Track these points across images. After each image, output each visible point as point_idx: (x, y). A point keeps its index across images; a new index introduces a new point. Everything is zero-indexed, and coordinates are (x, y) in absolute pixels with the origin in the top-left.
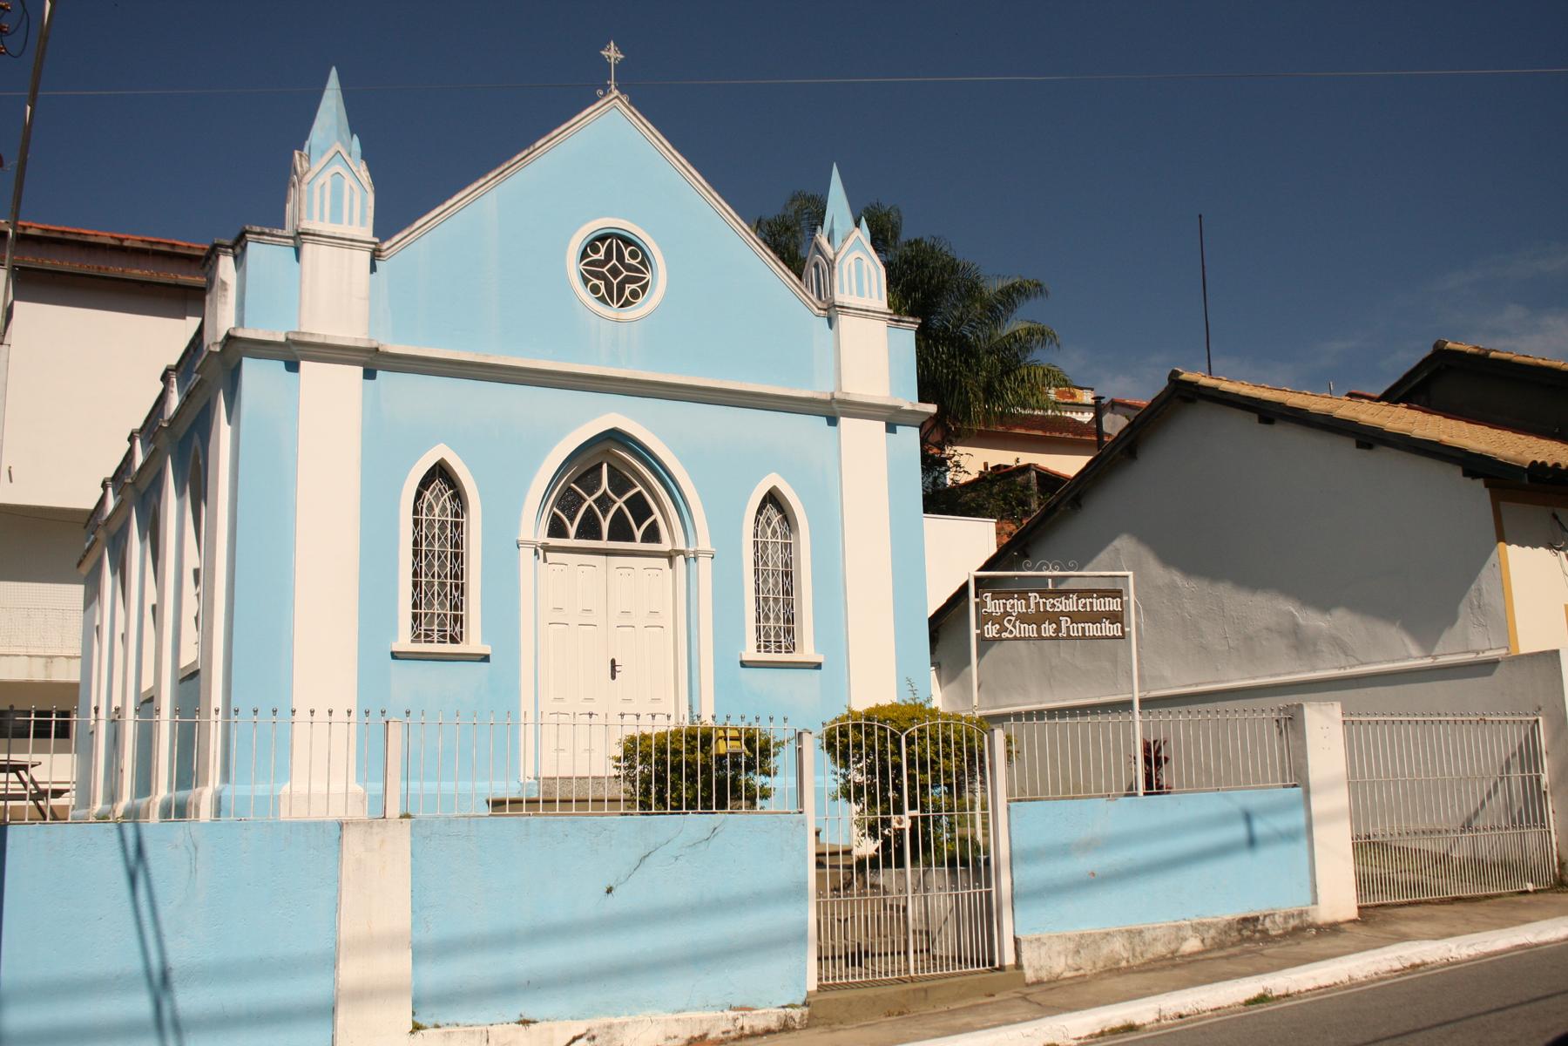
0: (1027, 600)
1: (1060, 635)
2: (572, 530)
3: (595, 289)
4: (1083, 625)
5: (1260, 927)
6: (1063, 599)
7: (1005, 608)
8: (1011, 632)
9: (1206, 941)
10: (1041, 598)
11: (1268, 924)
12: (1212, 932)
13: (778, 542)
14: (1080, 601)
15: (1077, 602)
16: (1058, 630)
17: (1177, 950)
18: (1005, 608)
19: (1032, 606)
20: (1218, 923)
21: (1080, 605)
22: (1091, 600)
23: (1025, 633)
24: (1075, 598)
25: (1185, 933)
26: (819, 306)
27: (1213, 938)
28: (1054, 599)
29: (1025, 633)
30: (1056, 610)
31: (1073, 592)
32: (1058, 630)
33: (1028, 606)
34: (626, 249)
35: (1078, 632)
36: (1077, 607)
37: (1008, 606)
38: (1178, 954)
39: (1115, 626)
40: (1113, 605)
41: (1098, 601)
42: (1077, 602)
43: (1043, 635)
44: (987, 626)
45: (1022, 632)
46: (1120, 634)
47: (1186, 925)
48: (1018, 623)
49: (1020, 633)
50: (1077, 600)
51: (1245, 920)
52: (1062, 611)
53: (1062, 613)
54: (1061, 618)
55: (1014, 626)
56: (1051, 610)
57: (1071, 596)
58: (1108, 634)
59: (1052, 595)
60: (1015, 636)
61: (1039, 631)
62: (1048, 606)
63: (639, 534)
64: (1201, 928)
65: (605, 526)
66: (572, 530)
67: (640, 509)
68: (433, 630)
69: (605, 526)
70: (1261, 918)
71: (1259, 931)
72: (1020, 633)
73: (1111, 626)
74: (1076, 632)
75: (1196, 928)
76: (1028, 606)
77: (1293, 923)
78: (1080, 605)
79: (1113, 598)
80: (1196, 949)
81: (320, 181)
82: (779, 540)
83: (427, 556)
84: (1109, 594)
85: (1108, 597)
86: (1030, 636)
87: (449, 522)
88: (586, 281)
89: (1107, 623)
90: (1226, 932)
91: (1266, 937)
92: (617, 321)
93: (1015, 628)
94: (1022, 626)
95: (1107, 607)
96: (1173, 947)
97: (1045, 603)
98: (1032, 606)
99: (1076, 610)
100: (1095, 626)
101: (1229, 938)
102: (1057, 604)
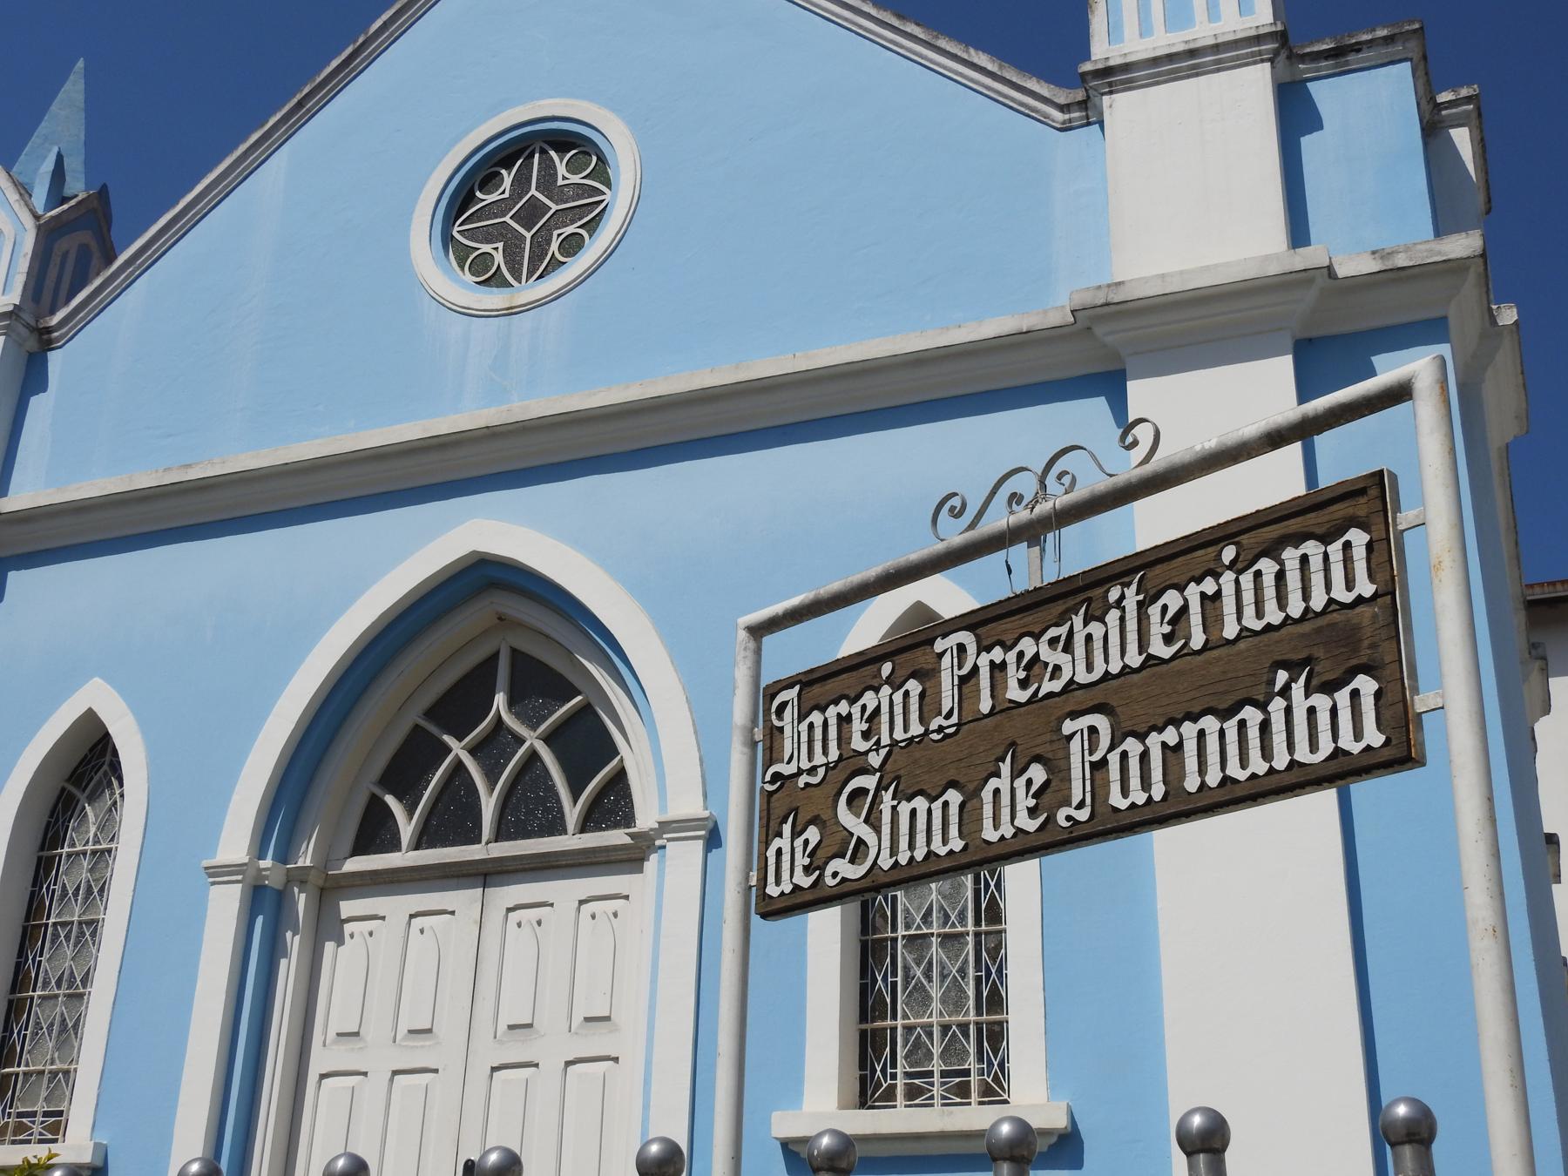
0: (928, 675)
2: (407, 829)
4: (1170, 736)
6: (1078, 621)
7: (843, 740)
10: (984, 648)
14: (1154, 611)
15: (1142, 619)
18: (843, 740)
21: (1158, 629)
23: (912, 846)
24: (1132, 599)
26: (1062, 100)
28: (1037, 637)
29: (912, 846)
30: (1048, 686)
31: (1119, 572)
32: (1048, 796)
34: (561, 161)
35: (1146, 784)
36: (1143, 645)
37: (858, 726)
39: (1343, 697)
41: (1247, 579)
42: (1142, 619)
45: (904, 843)
46: (1375, 738)
48: (887, 796)
49: (894, 851)
50: (1140, 604)
53: (1078, 699)
54: (1068, 727)
55: (872, 820)
56: (1023, 696)
57: (1114, 595)
58: (1303, 754)
59: (1028, 619)
61: (969, 816)
63: (572, 814)
65: (489, 806)
66: (407, 829)
68: (34, 1114)
69: (489, 806)
72: (894, 851)
73: (1321, 702)
78: (1158, 629)
79: (1326, 539)
84: (1293, 525)
85: (1298, 539)
88: (555, 264)
89: (1298, 689)
92: (510, 312)
93: (877, 830)
94: (905, 808)
95: (1271, 605)
100: (1231, 726)
102: (1050, 656)
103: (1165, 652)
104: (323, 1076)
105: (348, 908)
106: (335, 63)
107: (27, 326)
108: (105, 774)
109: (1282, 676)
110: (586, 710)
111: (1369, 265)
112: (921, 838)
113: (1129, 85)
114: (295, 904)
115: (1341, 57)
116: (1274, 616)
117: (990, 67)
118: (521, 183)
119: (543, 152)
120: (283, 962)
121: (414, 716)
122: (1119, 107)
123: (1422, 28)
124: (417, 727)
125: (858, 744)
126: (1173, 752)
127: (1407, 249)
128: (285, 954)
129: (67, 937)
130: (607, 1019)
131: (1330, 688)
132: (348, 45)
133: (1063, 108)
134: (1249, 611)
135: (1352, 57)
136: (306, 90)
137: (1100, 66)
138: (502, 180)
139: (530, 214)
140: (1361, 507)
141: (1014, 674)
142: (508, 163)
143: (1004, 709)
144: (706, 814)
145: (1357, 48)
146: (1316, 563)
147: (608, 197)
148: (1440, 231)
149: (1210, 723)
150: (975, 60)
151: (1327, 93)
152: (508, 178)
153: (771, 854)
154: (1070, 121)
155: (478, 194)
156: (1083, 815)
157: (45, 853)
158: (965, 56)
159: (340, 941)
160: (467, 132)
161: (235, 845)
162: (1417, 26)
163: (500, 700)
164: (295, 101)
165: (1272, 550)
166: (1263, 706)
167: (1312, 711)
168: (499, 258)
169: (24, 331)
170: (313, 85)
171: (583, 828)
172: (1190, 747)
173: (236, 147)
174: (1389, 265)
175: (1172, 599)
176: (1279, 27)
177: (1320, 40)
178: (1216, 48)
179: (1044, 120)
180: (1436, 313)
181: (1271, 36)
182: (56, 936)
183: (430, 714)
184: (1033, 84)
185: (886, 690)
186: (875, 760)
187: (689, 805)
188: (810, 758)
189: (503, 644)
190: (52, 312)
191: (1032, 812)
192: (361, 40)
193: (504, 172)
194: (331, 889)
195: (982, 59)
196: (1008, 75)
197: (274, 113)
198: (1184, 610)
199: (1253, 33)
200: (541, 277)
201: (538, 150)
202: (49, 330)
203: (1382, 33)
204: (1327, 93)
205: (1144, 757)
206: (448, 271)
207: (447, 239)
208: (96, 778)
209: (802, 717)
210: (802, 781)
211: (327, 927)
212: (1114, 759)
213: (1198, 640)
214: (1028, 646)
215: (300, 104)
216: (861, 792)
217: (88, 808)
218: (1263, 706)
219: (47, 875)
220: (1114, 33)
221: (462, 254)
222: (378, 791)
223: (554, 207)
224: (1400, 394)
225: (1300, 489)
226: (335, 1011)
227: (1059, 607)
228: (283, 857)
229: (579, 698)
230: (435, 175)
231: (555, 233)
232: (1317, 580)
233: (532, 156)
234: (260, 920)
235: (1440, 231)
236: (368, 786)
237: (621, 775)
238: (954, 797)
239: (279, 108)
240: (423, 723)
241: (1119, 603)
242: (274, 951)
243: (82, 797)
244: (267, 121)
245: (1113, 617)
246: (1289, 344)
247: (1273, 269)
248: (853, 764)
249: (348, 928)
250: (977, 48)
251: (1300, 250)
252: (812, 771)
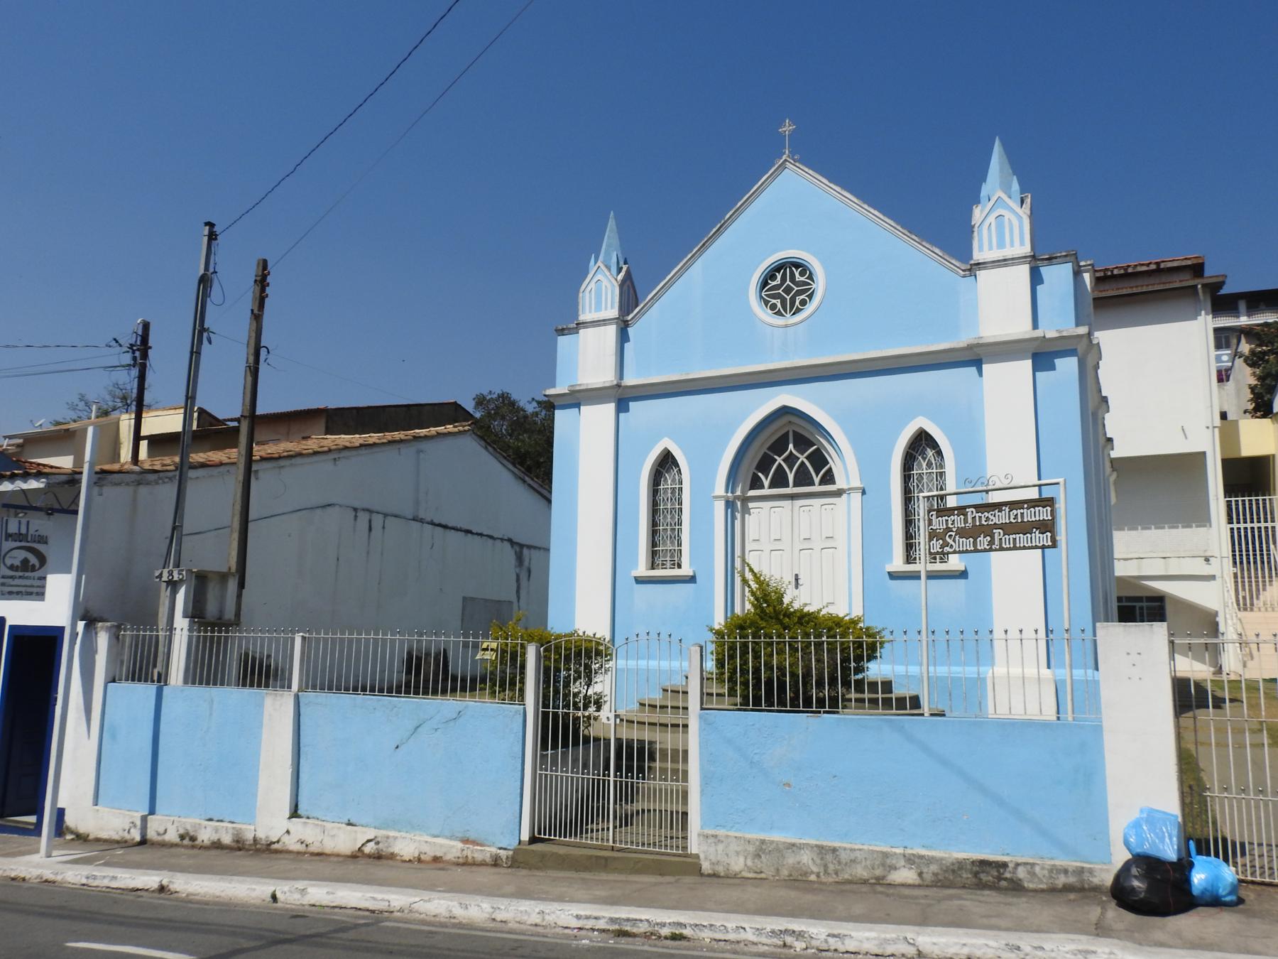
0: (965, 515)
1: (993, 547)
2: (766, 483)
3: (803, 303)
4: (1014, 536)
5: (1008, 875)
6: (997, 511)
7: (947, 524)
8: (952, 546)
9: (925, 875)
10: (977, 512)
11: (1021, 873)
12: (934, 868)
13: (933, 473)
14: (1011, 513)
16: (991, 543)
17: (884, 877)
18: (947, 524)
19: (970, 520)
20: (942, 859)
21: (1012, 517)
22: (1022, 511)
23: (963, 547)
24: (1007, 510)
25: (894, 862)
26: (963, 268)
27: (935, 874)
29: (963, 547)
30: (990, 523)
31: (1005, 504)
32: (991, 543)
33: (966, 521)
35: (1009, 544)
36: (1009, 519)
37: (950, 522)
38: (885, 882)
39: (1045, 535)
40: (1043, 514)
41: (1029, 511)
43: (1004, 546)
44: (979, 539)
45: (961, 546)
46: (1050, 543)
47: (895, 854)
48: (957, 537)
49: (959, 547)
50: (1009, 512)
51: (983, 863)
52: (995, 524)
53: (996, 526)
54: (994, 531)
55: (954, 541)
56: (985, 523)
57: (1004, 508)
58: (1038, 544)
60: (1043, 545)
61: (975, 544)
62: (983, 519)
63: (817, 480)
64: (916, 860)
65: (791, 477)
66: (766, 483)
67: (819, 460)
68: (666, 561)
69: (791, 477)
70: (1011, 865)
71: (1006, 879)
72: (959, 547)
73: (1041, 535)
74: (1007, 543)
75: (911, 860)
76: (966, 521)
77: (1062, 880)
78: (1012, 517)
79: (1044, 507)
80: (910, 882)
81: (589, 288)
82: (934, 471)
83: (663, 512)
85: (1038, 506)
86: (967, 550)
89: (1037, 532)
90: (953, 871)
91: (1016, 887)
92: (786, 326)
93: (955, 542)
94: (961, 540)
96: (878, 872)
97: (980, 517)
98: (970, 520)
99: (1008, 522)
100: (1025, 536)
101: (959, 879)
102: (992, 517)
103: (1014, 521)
104: (750, 551)
105: (751, 505)
106: (714, 230)
107: (622, 321)
109: (1034, 530)
110: (818, 449)
111: (1055, 335)
112: (965, 546)
113: (985, 268)
114: (737, 505)
115: (1050, 260)
116: (1034, 519)
117: (940, 254)
118: (784, 279)
119: (790, 268)
120: (736, 521)
121: (764, 450)
122: (982, 274)
123: (1076, 253)
124: (765, 453)
125: (950, 526)
126: (1015, 539)
127: (1066, 330)
128: (736, 519)
129: (667, 512)
130: (832, 537)
131: (1043, 533)
133: (963, 270)
134: (1029, 517)
135: (1054, 260)
136: (705, 240)
137: (976, 262)
139: (788, 290)
140: (1049, 503)
141: (983, 519)
143: (981, 525)
144: (862, 486)
145: (1056, 258)
146: (1041, 511)
147: (814, 286)
148: (1077, 325)
149: (1021, 535)
150: (935, 251)
151: (1046, 271)
152: (779, 276)
153: (931, 544)
155: (769, 281)
156: (998, 547)
159: (750, 514)
160: (765, 259)
161: (720, 489)
162: (1074, 252)
163: (791, 446)
165: (1034, 507)
166: (1031, 534)
167: (1039, 537)
168: (779, 305)
169: (620, 322)
171: (820, 484)
172: (1018, 539)
173: (683, 259)
174: (1061, 335)
175: (1015, 512)
176: (1032, 254)
177: (1045, 255)
178: (1013, 259)
179: (957, 273)
180: (1075, 347)
181: (1030, 256)
182: (663, 512)
183: (769, 449)
184: (953, 262)
185: (956, 516)
186: (954, 530)
187: (856, 483)
188: (939, 526)
189: (791, 429)
190: (628, 315)
191: (988, 545)
192: (723, 222)
193: (777, 274)
194: (745, 500)
195: (937, 251)
196: (945, 257)
198: (1017, 514)
199: (1024, 255)
200: (794, 314)
202: (628, 321)
203: (1064, 254)
204: (1046, 271)
205: (1009, 539)
206: (761, 307)
207: (761, 297)
208: (667, 466)
209: (937, 518)
210: (938, 531)
211: (746, 511)
212: (1003, 538)
213: (1019, 520)
214: (986, 514)
215: (704, 244)
216: (952, 535)
217: (666, 475)
218: (1031, 534)
219: (657, 494)
220: (981, 249)
221: (766, 303)
222: (756, 472)
224: (1058, 484)
225: (1037, 497)
226: (751, 533)
227: (992, 508)
228: (732, 493)
229: (815, 447)
230: (755, 276)
231: (797, 298)
232: (1041, 515)
233: (786, 269)
234: (729, 510)
235: (1077, 325)
236: (753, 470)
237: (830, 469)
238: (971, 540)
239: (697, 245)
240: (767, 451)
241: (1005, 510)
242: (733, 518)
243: (664, 472)
244: (693, 250)
245: (1003, 512)
246: (1030, 356)
247: (1027, 336)
248: (948, 530)
249: (751, 510)
250: (935, 246)
251: (1036, 331)
252: (940, 529)
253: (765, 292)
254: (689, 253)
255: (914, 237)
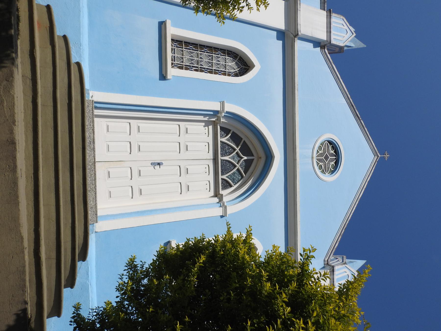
34: (333, 163)
63: (224, 177)
65: (227, 158)
68: (174, 54)
69: (227, 158)
81: (345, 24)
83: (209, 56)
87: (225, 70)
92: (312, 158)
104: (179, 125)
105: (211, 127)
106: (358, 113)
107: (327, 44)
108: (240, 66)
119: (336, 158)
120: (203, 117)
121: (244, 139)
129: (210, 59)
132: (360, 116)
133: (328, 260)
136: (355, 107)
138: (332, 151)
142: (335, 152)
147: (327, 174)
154: (325, 261)
157: (226, 52)
158: (338, 242)
159: (204, 126)
163: (245, 158)
164: (353, 105)
170: (355, 109)
179: (326, 257)
190: (328, 50)
192: (360, 119)
194: (214, 124)
195: (337, 245)
197: (352, 100)
201: (336, 157)
202: (324, 48)
211: (207, 124)
215: (352, 106)
219: (222, 52)
222: (231, 132)
223: (327, 162)
226: (192, 127)
229: (244, 175)
233: (335, 156)
234: (212, 113)
242: (205, 115)
243: (236, 61)
244: (351, 99)
249: (207, 128)
253: (327, 143)
254: (350, 96)
255: (343, 231)
